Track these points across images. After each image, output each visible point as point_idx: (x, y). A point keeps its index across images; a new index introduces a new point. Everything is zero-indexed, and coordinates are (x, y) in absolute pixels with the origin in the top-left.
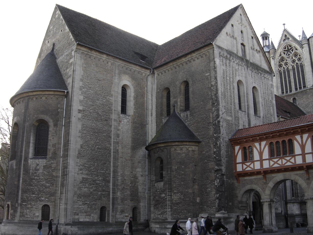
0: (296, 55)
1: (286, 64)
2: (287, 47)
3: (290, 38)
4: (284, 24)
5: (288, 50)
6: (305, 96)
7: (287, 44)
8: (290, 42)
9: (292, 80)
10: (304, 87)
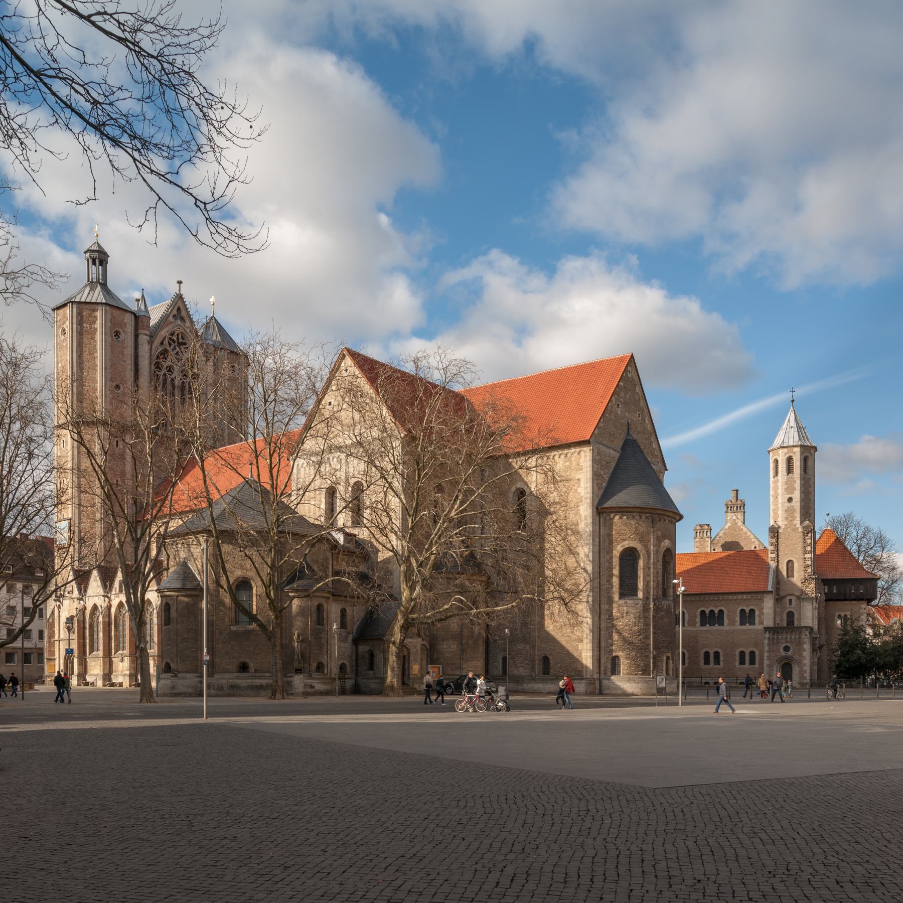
4: (180, 282)
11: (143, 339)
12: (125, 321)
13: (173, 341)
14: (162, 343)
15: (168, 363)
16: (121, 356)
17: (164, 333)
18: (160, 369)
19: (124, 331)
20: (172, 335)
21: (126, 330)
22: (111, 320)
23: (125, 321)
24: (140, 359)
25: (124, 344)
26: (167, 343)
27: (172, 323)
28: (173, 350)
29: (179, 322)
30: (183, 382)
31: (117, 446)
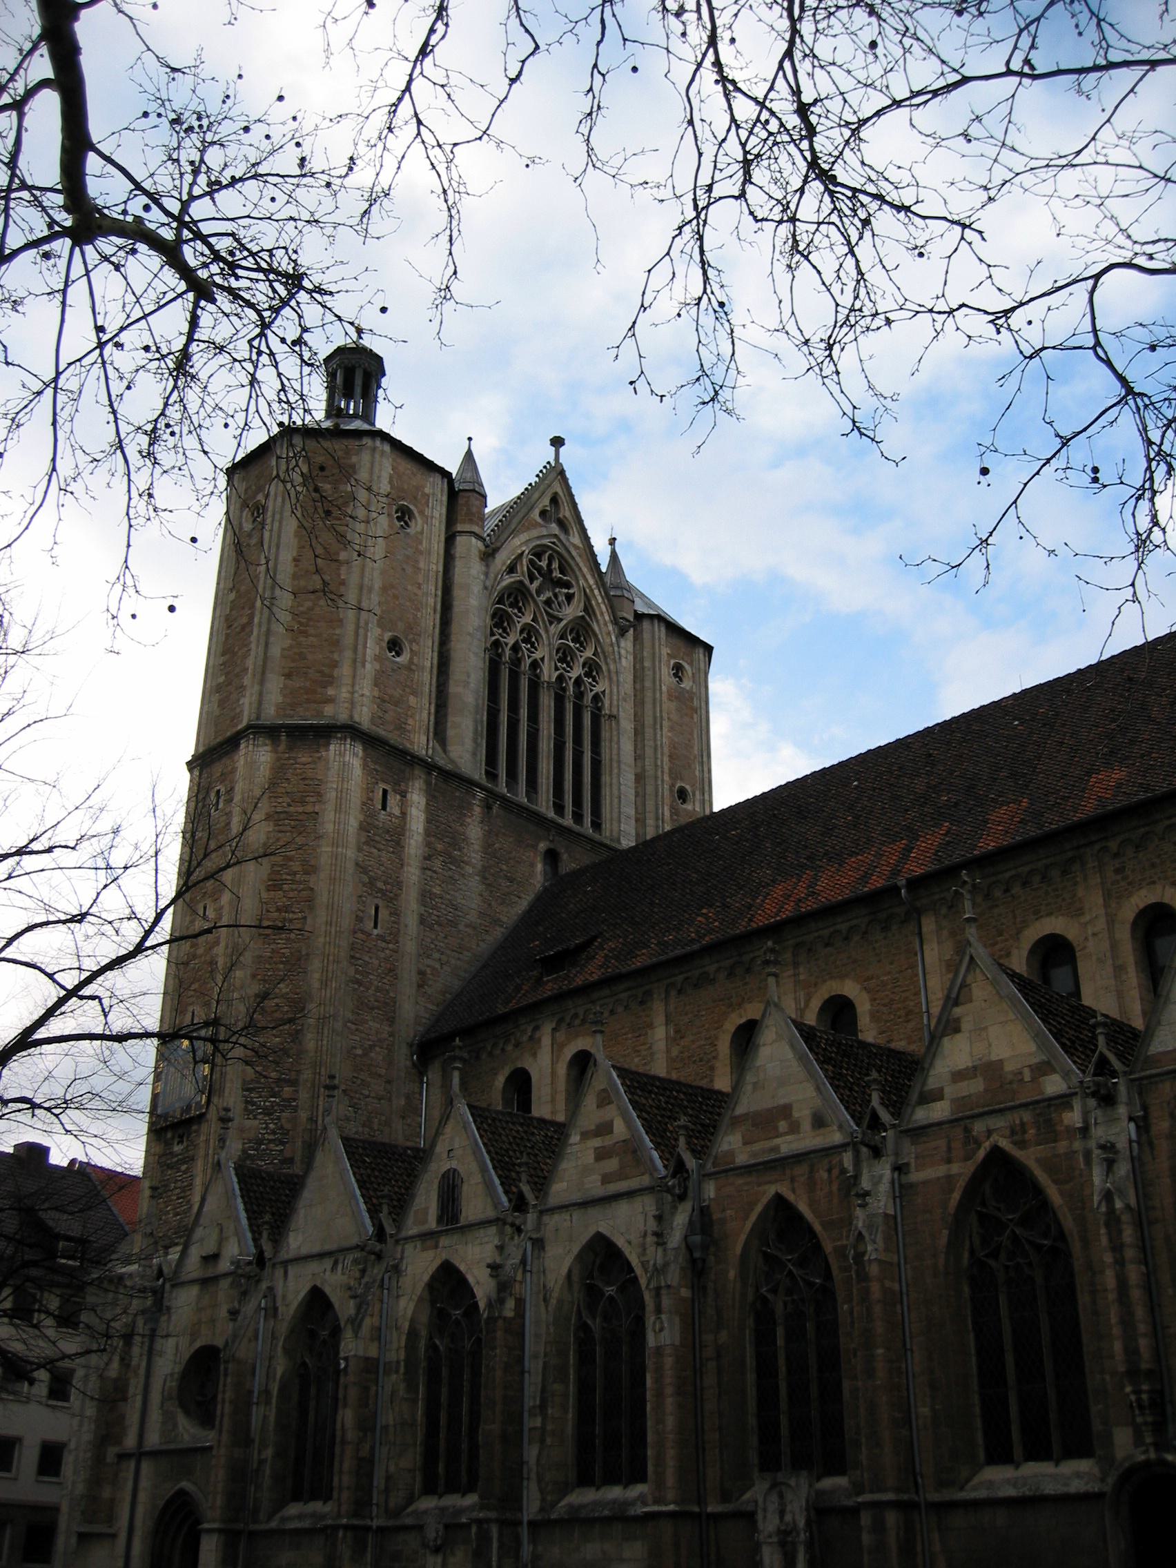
0: (581, 630)
3: (574, 530)
4: (557, 442)
7: (553, 543)
8: (574, 553)
11: (469, 547)
12: (427, 490)
13: (539, 569)
14: (511, 569)
15: (527, 619)
16: (409, 570)
17: (519, 544)
18: (505, 630)
19: (422, 513)
20: (539, 555)
21: (428, 512)
22: (391, 477)
23: (427, 490)
24: (457, 593)
25: (421, 543)
26: (525, 569)
27: (536, 525)
28: (539, 592)
29: (554, 528)
30: (561, 678)
31: (384, 807)
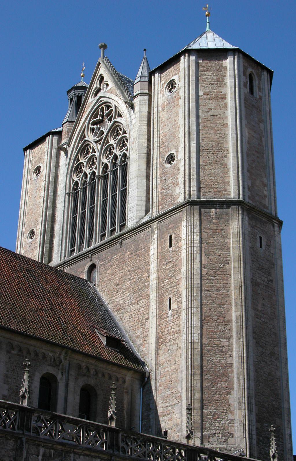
1: (91, 161)
2: (100, 113)
5: (101, 122)
6: (116, 257)
9: (98, 210)
10: (122, 226)
